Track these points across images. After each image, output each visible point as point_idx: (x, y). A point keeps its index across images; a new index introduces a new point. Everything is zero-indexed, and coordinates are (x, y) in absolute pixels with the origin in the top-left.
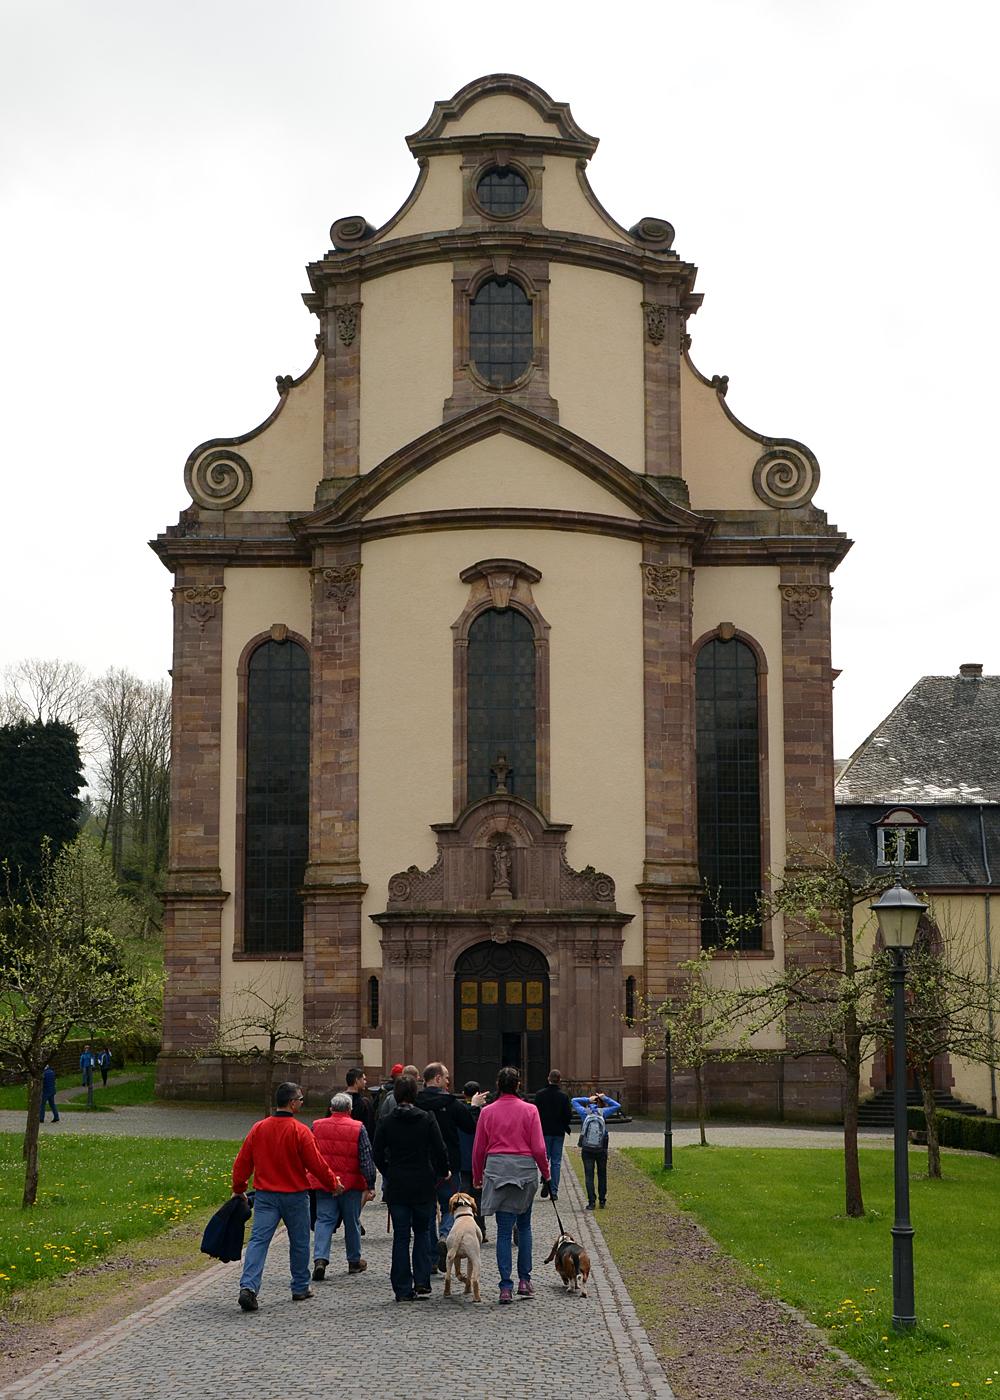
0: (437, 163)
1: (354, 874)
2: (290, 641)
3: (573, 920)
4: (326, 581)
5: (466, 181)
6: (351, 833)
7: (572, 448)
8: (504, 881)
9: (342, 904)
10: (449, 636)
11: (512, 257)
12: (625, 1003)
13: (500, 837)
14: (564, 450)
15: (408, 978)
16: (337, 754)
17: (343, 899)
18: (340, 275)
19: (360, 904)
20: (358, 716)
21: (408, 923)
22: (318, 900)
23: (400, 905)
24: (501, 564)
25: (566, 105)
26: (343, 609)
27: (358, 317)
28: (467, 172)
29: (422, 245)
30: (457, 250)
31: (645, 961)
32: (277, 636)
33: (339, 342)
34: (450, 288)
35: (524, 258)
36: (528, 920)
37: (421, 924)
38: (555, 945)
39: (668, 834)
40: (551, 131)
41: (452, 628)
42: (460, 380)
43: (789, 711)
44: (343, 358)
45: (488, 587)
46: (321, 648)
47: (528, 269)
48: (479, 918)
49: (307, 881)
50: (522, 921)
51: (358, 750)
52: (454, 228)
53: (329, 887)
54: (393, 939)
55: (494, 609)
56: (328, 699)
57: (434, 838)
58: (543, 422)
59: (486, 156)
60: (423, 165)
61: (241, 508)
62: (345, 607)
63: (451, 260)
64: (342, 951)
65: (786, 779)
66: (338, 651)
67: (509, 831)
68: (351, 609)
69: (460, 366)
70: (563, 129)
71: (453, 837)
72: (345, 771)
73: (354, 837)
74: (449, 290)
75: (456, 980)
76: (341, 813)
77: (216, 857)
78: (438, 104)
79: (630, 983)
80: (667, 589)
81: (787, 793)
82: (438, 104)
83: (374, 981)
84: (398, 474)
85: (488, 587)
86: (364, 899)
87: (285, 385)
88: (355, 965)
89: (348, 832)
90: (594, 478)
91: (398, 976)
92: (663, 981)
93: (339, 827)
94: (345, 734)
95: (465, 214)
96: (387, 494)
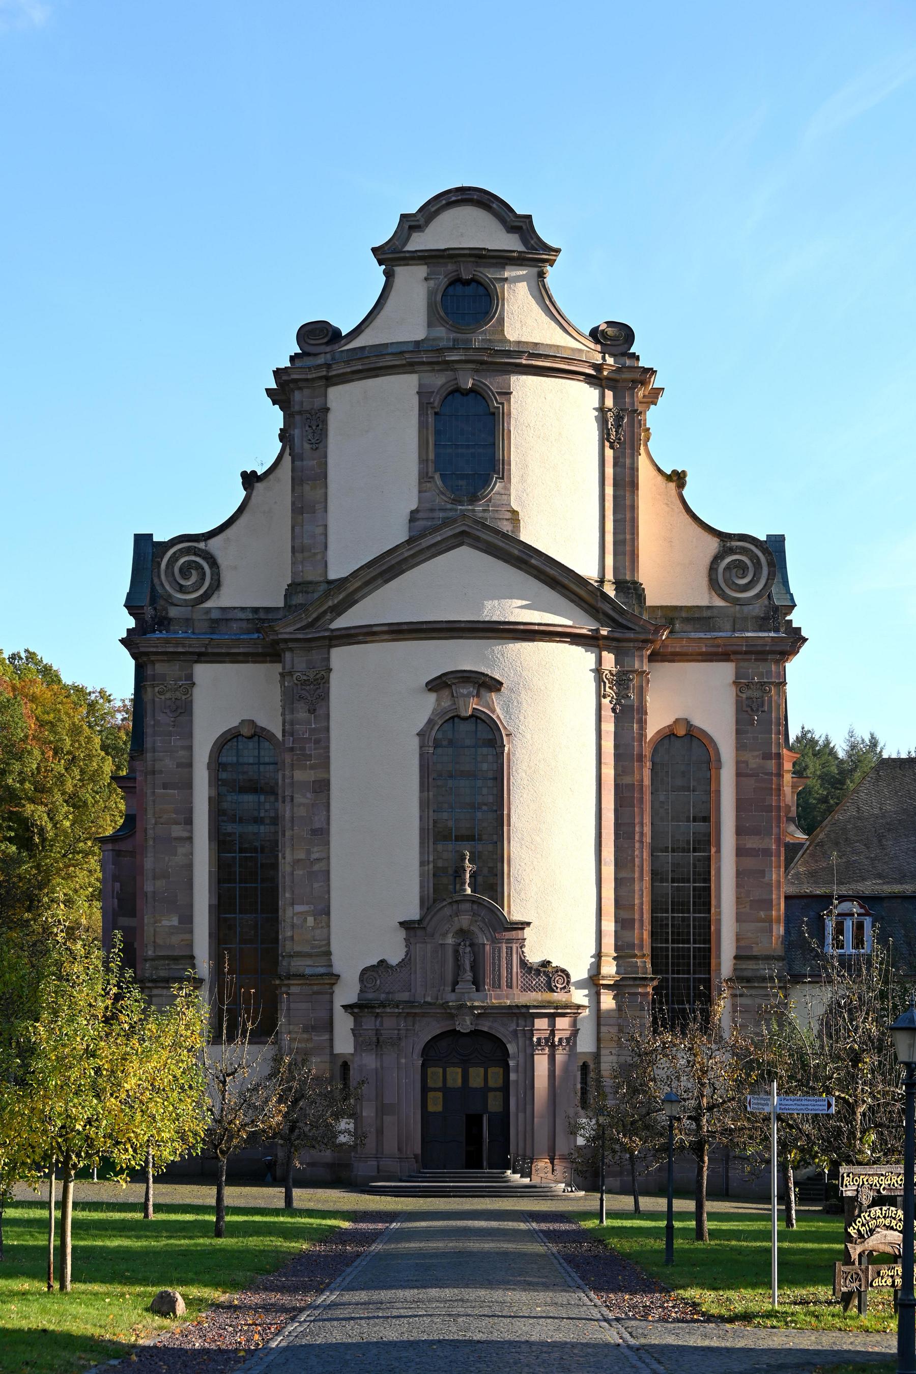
0: (399, 270)
1: (325, 966)
2: (259, 734)
4: (297, 685)
5: (431, 294)
6: (322, 927)
7: (533, 561)
8: (469, 976)
9: (315, 993)
10: (415, 742)
11: (476, 371)
12: (579, 1086)
13: (462, 933)
14: (526, 562)
15: (379, 1064)
16: (309, 852)
17: (315, 988)
18: (307, 380)
19: (332, 994)
20: (329, 816)
21: (378, 1013)
22: (294, 990)
23: (370, 996)
24: (465, 675)
25: (529, 217)
26: (312, 711)
27: (325, 422)
28: (432, 283)
29: (388, 358)
30: (423, 363)
31: (599, 1048)
32: (246, 731)
33: (307, 446)
34: (415, 401)
35: (488, 371)
36: (490, 1011)
37: (392, 1015)
38: (515, 1032)
39: (622, 928)
40: (511, 243)
41: (417, 734)
42: (425, 491)
43: (741, 805)
44: (310, 463)
45: (453, 696)
46: (292, 749)
47: (492, 383)
48: (445, 1009)
49: (282, 971)
50: (489, 1013)
51: (329, 848)
52: (420, 339)
53: (302, 976)
54: (364, 1027)
55: (458, 716)
56: (299, 799)
57: (402, 934)
58: (505, 536)
59: (450, 267)
60: (389, 274)
61: (209, 604)
62: (315, 710)
63: (415, 372)
64: (316, 1038)
65: (737, 870)
66: (308, 753)
67: (472, 928)
68: (321, 712)
69: (424, 477)
70: (525, 242)
71: (420, 933)
72: (316, 868)
73: (325, 930)
74: (414, 402)
75: (423, 1065)
76: (312, 906)
77: (190, 945)
78: (404, 217)
79: (584, 1068)
80: (623, 693)
81: (738, 886)
82: (404, 217)
83: (345, 1066)
84: (367, 583)
85: (453, 696)
86: (337, 990)
87: (249, 479)
88: (327, 1051)
89: (320, 926)
90: (553, 588)
91: (370, 1061)
93: (310, 920)
94: (314, 832)
95: (430, 325)
96: (356, 602)
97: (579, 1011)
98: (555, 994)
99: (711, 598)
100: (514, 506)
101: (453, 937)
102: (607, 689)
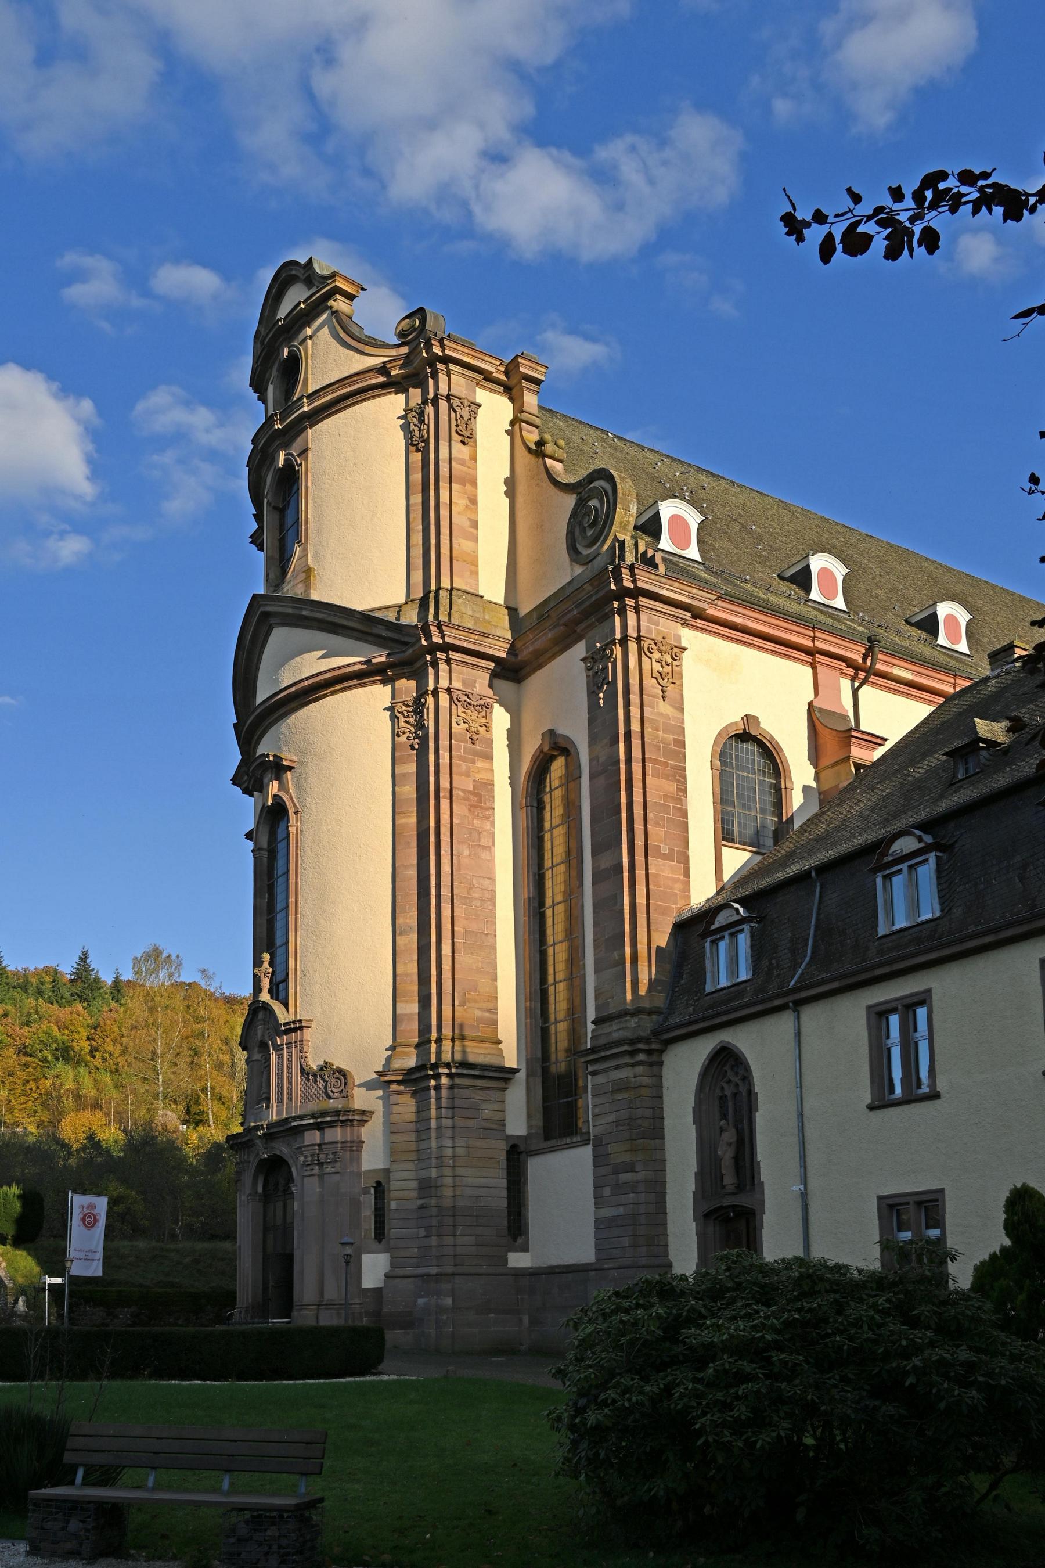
3: (293, 1124)
7: (304, 613)
90: (337, 634)
92: (414, 1184)
97: (365, 1118)
98: (331, 1101)
99: (572, 570)
100: (310, 563)
101: (259, 1052)
102: (402, 724)
